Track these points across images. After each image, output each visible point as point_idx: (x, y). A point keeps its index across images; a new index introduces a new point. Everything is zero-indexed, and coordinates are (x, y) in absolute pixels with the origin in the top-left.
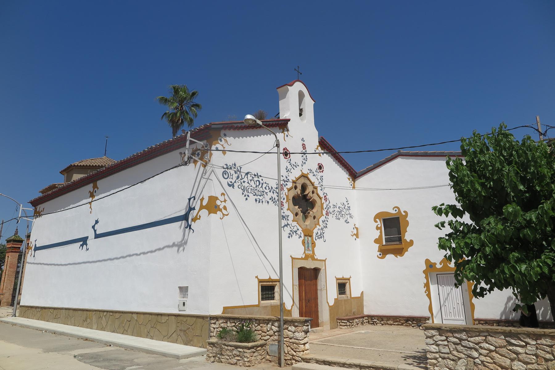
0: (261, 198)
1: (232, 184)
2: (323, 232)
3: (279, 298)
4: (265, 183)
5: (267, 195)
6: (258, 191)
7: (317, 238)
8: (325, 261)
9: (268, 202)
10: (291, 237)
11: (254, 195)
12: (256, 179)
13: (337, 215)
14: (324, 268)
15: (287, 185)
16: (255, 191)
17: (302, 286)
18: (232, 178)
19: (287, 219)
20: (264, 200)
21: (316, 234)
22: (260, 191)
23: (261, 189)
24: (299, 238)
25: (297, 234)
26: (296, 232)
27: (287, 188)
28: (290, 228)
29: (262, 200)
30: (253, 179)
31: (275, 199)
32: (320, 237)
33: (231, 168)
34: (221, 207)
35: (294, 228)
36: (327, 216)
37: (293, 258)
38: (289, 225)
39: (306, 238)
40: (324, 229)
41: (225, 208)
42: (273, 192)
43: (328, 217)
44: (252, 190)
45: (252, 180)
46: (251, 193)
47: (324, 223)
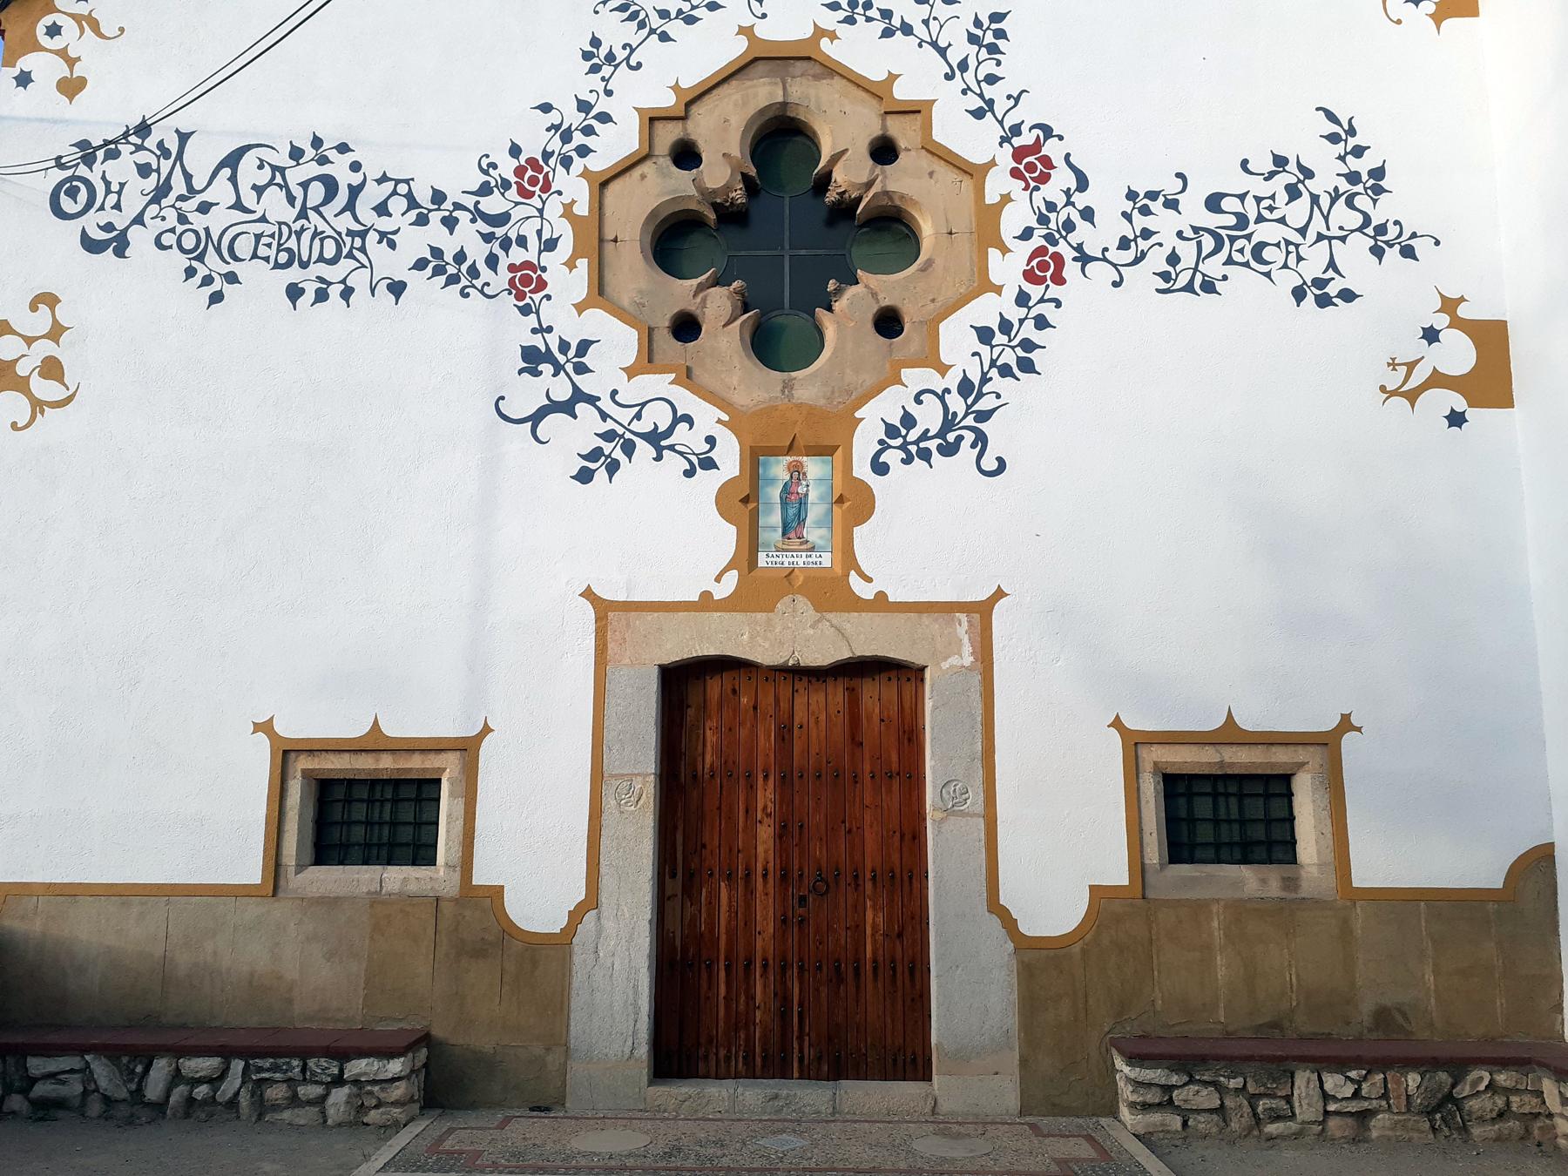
0: (333, 273)
1: (115, 233)
2: (984, 404)
3: (456, 853)
4: (384, 179)
5: (392, 245)
6: (316, 234)
7: (892, 457)
8: (982, 611)
9: (397, 288)
10: (601, 475)
11: (277, 266)
12: (295, 176)
13: (1173, 259)
14: (968, 660)
15: (583, 151)
16: (292, 244)
17: (751, 787)
18: (117, 207)
19: (569, 367)
20: (359, 280)
21: (891, 431)
22: (330, 232)
23: (345, 222)
24: (689, 473)
25: (671, 448)
26: (654, 438)
27: (586, 174)
28: (604, 416)
29: (343, 281)
30: (279, 179)
31: (460, 257)
32: (932, 445)
33: (113, 155)
34: (22, 369)
35: (638, 416)
36: (1035, 292)
37: (604, 609)
38: (592, 400)
39: (779, 469)
40: (997, 382)
41: (51, 368)
42: (450, 223)
43: (1054, 291)
44: (264, 240)
45: (270, 183)
46: (255, 256)
47: (1000, 338)
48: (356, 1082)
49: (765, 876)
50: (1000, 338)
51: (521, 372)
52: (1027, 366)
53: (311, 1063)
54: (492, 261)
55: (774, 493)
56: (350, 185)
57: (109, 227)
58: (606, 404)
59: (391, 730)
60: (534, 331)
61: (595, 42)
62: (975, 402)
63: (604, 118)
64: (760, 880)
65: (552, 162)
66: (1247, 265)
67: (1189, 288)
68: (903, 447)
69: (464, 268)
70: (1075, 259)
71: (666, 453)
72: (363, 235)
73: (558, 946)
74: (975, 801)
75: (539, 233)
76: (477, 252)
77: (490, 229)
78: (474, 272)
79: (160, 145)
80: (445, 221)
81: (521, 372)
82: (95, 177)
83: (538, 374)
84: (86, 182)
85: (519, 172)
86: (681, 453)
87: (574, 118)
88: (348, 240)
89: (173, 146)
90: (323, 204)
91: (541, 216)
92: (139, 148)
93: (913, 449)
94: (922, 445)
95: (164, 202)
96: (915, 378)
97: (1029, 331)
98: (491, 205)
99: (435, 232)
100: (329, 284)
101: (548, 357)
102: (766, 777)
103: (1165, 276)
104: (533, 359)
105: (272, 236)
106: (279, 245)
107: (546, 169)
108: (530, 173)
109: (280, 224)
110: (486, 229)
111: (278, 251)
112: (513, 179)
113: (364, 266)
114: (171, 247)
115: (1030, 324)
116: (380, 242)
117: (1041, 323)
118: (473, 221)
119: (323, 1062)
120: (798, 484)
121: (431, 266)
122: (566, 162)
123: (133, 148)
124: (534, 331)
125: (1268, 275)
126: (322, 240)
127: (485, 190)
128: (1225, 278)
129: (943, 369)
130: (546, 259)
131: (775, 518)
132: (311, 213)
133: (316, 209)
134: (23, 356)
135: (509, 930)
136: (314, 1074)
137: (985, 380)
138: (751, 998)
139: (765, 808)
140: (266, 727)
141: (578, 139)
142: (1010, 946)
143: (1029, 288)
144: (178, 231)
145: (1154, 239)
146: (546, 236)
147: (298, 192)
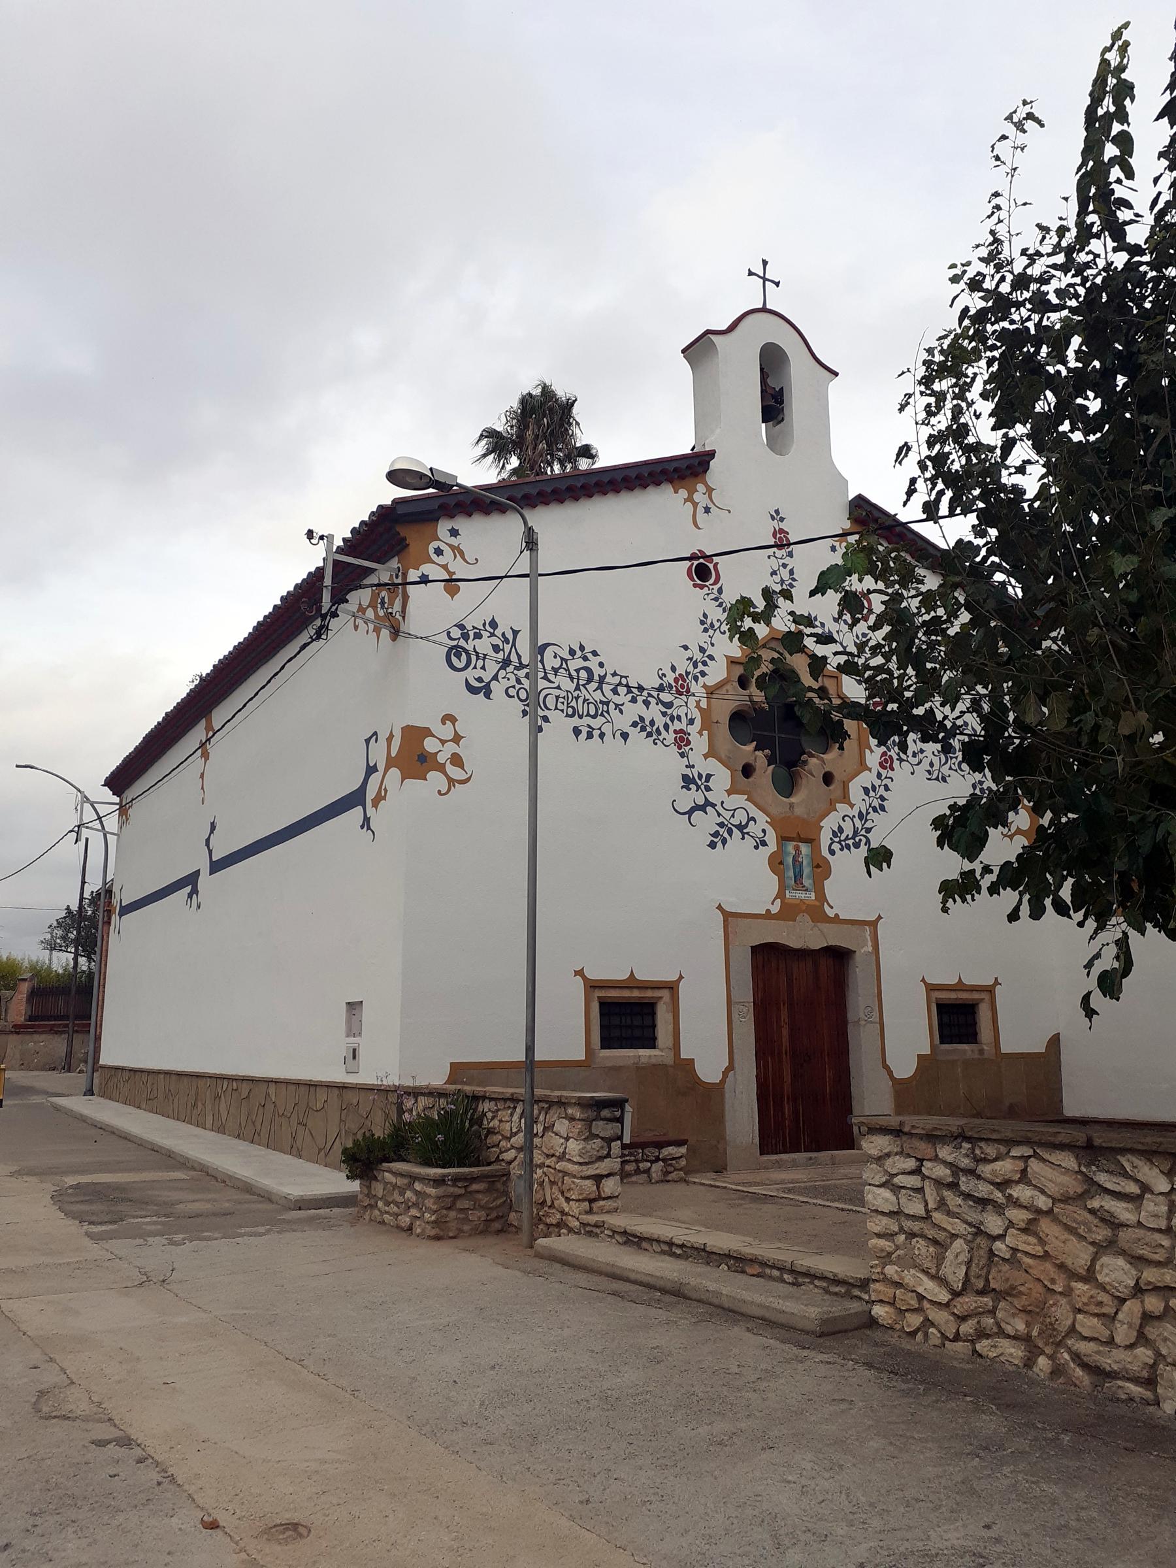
0: (596, 723)
1: (484, 684)
2: (869, 825)
3: (670, 1043)
4: (614, 674)
5: (621, 712)
6: (585, 700)
7: (836, 847)
8: (874, 924)
9: (625, 736)
10: (719, 845)
11: (568, 716)
12: (574, 664)
13: (932, 765)
14: (870, 949)
15: (703, 674)
16: (574, 704)
17: (779, 1009)
18: (483, 668)
19: (703, 787)
20: (607, 729)
21: (835, 834)
22: (591, 700)
23: (598, 696)
24: (756, 847)
25: (748, 833)
26: (740, 827)
27: (705, 686)
28: (719, 815)
29: (600, 729)
30: (564, 666)
31: (652, 723)
32: (850, 842)
33: (478, 636)
34: (441, 758)
35: (733, 816)
36: (884, 773)
37: (727, 916)
38: (713, 805)
39: (790, 847)
40: (872, 815)
41: (457, 760)
42: (647, 703)
43: (891, 774)
44: (561, 700)
45: (560, 667)
46: (556, 708)
47: (872, 794)
48: (664, 1160)
49: (786, 1053)
50: (872, 794)
51: (682, 787)
52: (883, 808)
53: (646, 1151)
54: (666, 727)
55: (790, 860)
56: (599, 675)
57: (480, 680)
58: (719, 808)
59: (640, 976)
60: (687, 767)
61: (705, 616)
62: (865, 823)
63: (711, 658)
64: (784, 1056)
65: (690, 677)
66: (956, 771)
67: (937, 779)
68: (839, 842)
69: (654, 728)
70: (897, 759)
71: (746, 836)
72: (607, 704)
73: (719, 1088)
74: (876, 1014)
75: (686, 714)
76: (660, 721)
77: (665, 710)
78: (658, 732)
79: (503, 634)
80: (644, 702)
81: (682, 787)
82: (469, 647)
83: (690, 789)
84: (467, 652)
85: (676, 680)
86: (752, 837)
87: (698, 656)
88: (601, 706)
89: (510, 636)
90: (586, 684)
91: (687, 706)
92: (492, 635)
93: (843, 843)
94: (847, 842)
95: (508, 669)
96: (842, 809)
97: (882, 791)
98: (666, 697)
99: (639, 708)
100: (593, 729)
101: (693, 781)
102: (784, 1004)
103: (929, 772)
104: (688, 781)
105: (564, 698)
106: (568, 704)
107: (688, 681)
108: (680, 682)
109: (567, 691)
110: (664, 710)
111: (568, 707)
112: (674, 684)
113: (609, 722)
114: (513, 697)
115: (882, 787)
116: (615, 709)
117: (887, 788)
118: (657, 704)
119: (651, 1149)
120: (799, 857)
121: (640, 725)
122: (696, 679)
123: (489, 635)
124: (687, 767)
125: (963, 776)
126: (588, 704)
127: (661, 689)
128: (949, 776)
129: (852, 806)
130: (690, 729)
131: (791, 873)
132: (582, 688)
133: (584, 685)
134: (440, 751)
135: (697, 1081)
136: (647, 1156)
137: (868, 813)
138: (783, 1113)
139: (784, 1020)
140: (580, 973)
141: (701, 667)
142: (890, 1083)
143: (881, 770)
144: (517, 688)
145: (924, 754)
146: (689, 717)
147: (574, 674)
